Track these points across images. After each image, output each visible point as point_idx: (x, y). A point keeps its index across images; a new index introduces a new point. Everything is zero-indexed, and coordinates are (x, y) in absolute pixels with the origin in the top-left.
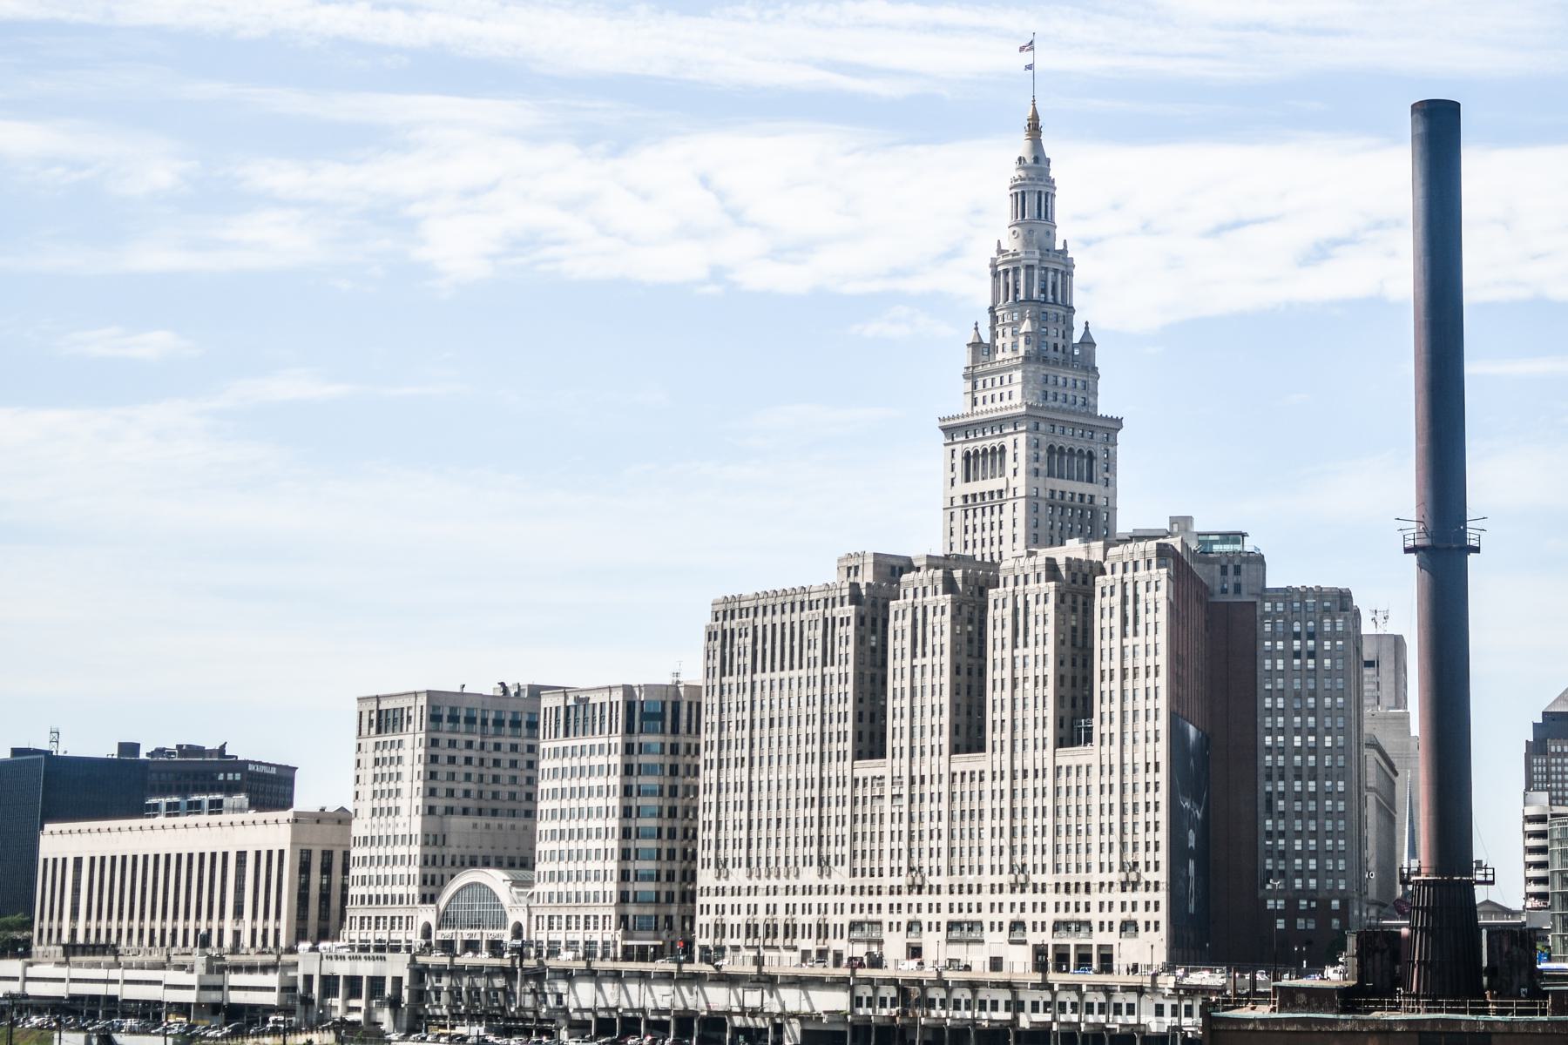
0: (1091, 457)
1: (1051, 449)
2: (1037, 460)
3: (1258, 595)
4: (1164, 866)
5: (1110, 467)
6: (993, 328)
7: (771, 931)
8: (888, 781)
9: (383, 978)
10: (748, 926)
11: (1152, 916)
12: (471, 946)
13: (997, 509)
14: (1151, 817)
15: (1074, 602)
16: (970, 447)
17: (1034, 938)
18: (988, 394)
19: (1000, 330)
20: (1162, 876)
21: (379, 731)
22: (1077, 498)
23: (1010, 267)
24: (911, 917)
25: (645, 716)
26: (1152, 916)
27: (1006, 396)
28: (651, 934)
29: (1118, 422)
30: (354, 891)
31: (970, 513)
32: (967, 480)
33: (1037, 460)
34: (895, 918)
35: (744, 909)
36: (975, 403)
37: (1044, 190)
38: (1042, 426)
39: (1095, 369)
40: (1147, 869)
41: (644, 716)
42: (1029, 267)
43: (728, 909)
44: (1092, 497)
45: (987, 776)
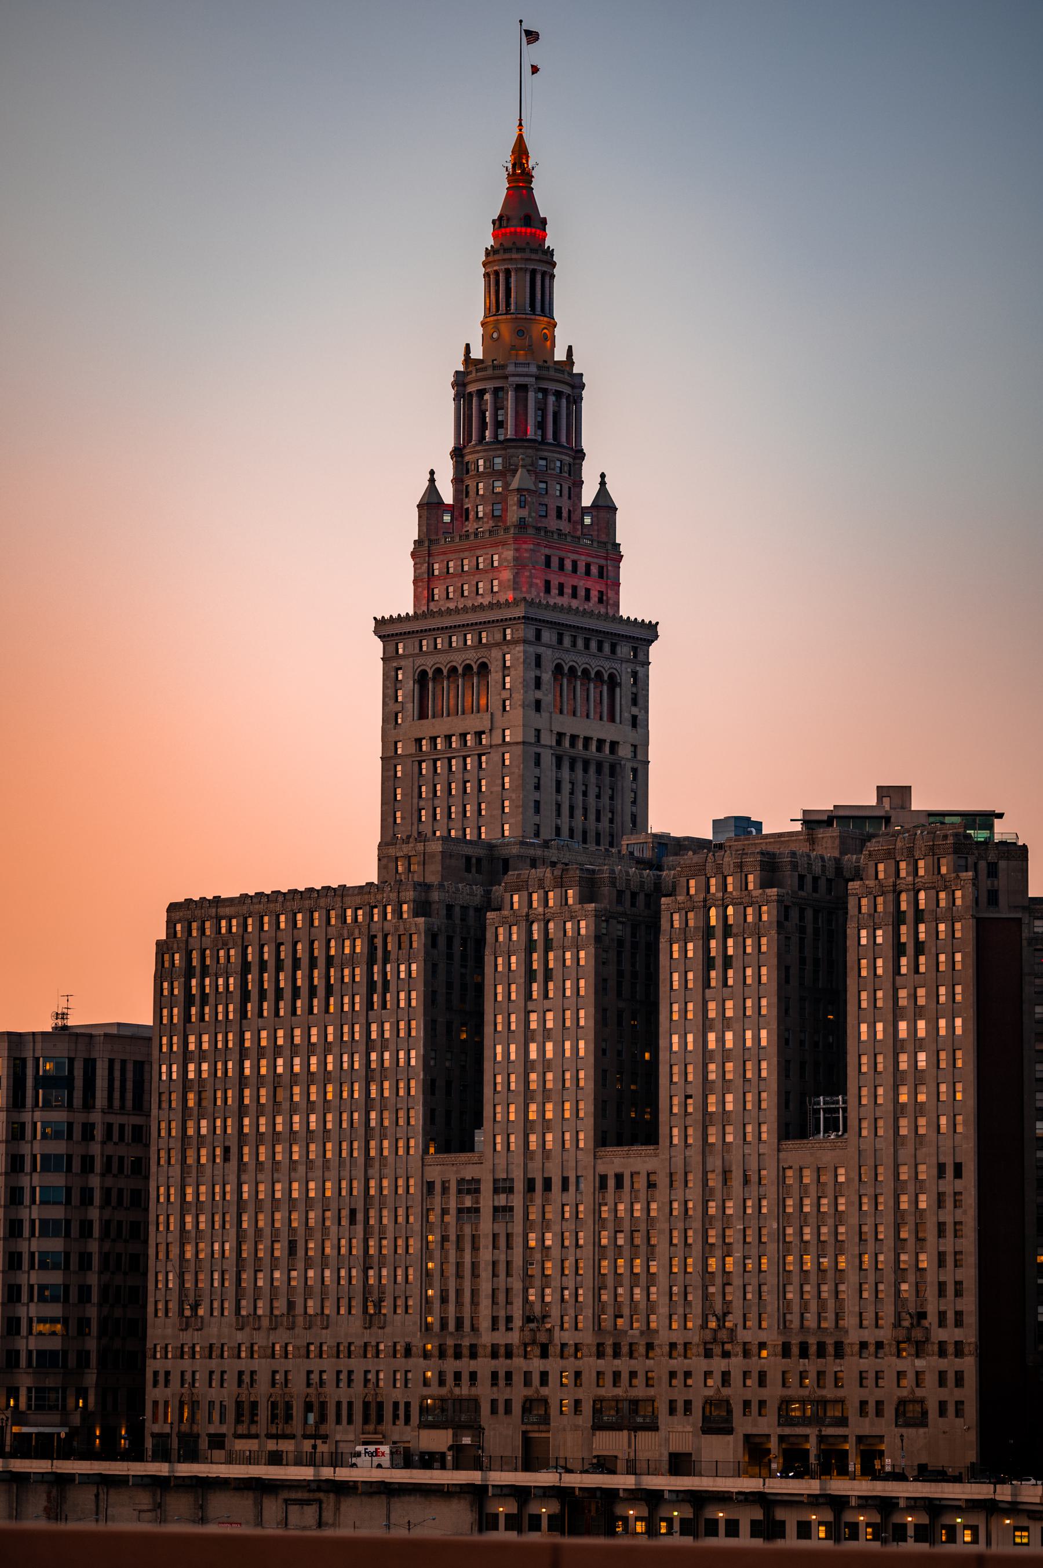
0: (613, 683)
1: (558, 668)
2: (538, 683)
3: (1024, 908)
4: (971, 1319)
5: (639, 698)
6: (457, 481)
7: (281, 1412)
8: (486, 1188)
11: (951, 1394)
14: (948, 1245)
15: (802, 918)
16: (429, 664)
19: (471, 483)
20: (969, 1334)
23: (490, 385)
24: (529, 1392)
25: (44, 1082)
26: (951, 1394)
28: (56, 1418)
29: (648, 632)
32: (423, 715)
33: (538, 683)
34: (502, 1394)
38: (547, 636)
40: (942, 1323)
44: (614, 745)
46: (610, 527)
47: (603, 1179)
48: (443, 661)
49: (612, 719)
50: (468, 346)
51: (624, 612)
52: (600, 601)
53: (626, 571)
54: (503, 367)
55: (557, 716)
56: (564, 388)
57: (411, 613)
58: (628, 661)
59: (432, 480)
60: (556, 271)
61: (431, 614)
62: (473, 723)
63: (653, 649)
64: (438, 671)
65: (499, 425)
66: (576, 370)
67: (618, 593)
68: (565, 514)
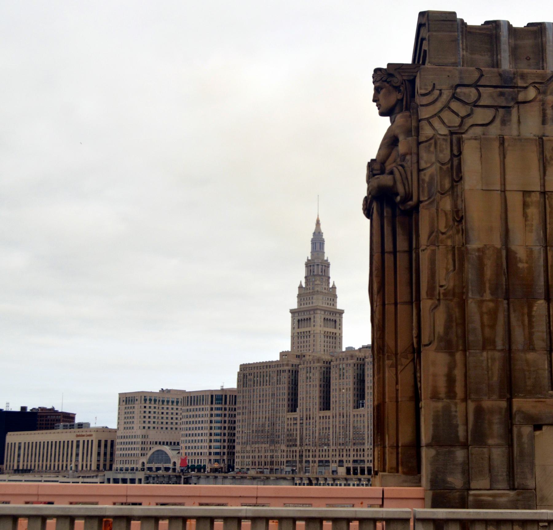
5: (341, 324)
6: (306, 283)
8: (298, 419)
9: (135, 479)
10: (252, 462)
12: (158, 469)
13: (308, 337)
16: (300, 318)
17: (346, 465)
18: (305, 302)
21: (126, 404)
30: (118, 453)
35: (251, 457)
36: (301, 305)
41: (216, 399)
42: (318, 265)
43: (245, 457)
45: (331, 417)
47: (320, 417)
48: (303, 317)
49: (335, 328)
53: (339, 300)
56: (326, 265)
62: (307, 329)
63: (344, 315)
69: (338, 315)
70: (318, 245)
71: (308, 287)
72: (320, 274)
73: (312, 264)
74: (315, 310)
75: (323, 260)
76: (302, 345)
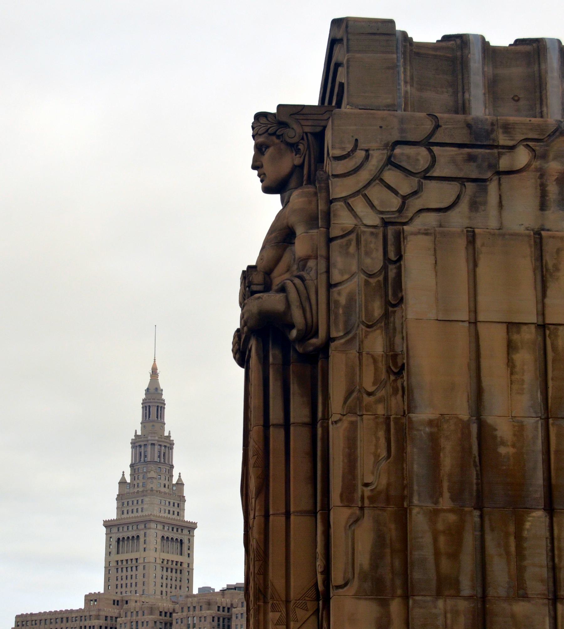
1: (163, 537)
5: (190, 548)
13: (134, 569)
16: (121, 536)
22: (174, 563)
27: (140, 510)
31: (120, 570)
37: (160, 405)
39: (184, 497)
42: (153, 444)
46: (182, 490)
48: (125, 535)
49: (181, 554)
50: (136, 431)
51: (186, 519)
52: (178, 515)
53: (187, 505)
54: (147, 437)
55: (162, 554)
56: (167, 445)
57: (115, 518)
58: (187, 535)
59: (123, 475)
60: (165, 406)
61: (122, 519)
62: (133, 556)
63: (196, 532)
64: (124, 538)
65: (145, 456)
66: (171, 439)
67: (184, 512)
68: (167, 486)
69: (186, 532)
70: (153, 410)
71: (135, 483)
72: (157, 459)
73: (142, 444)
74: (146, 522)
75: (162, 436)
76: (124, 582)
